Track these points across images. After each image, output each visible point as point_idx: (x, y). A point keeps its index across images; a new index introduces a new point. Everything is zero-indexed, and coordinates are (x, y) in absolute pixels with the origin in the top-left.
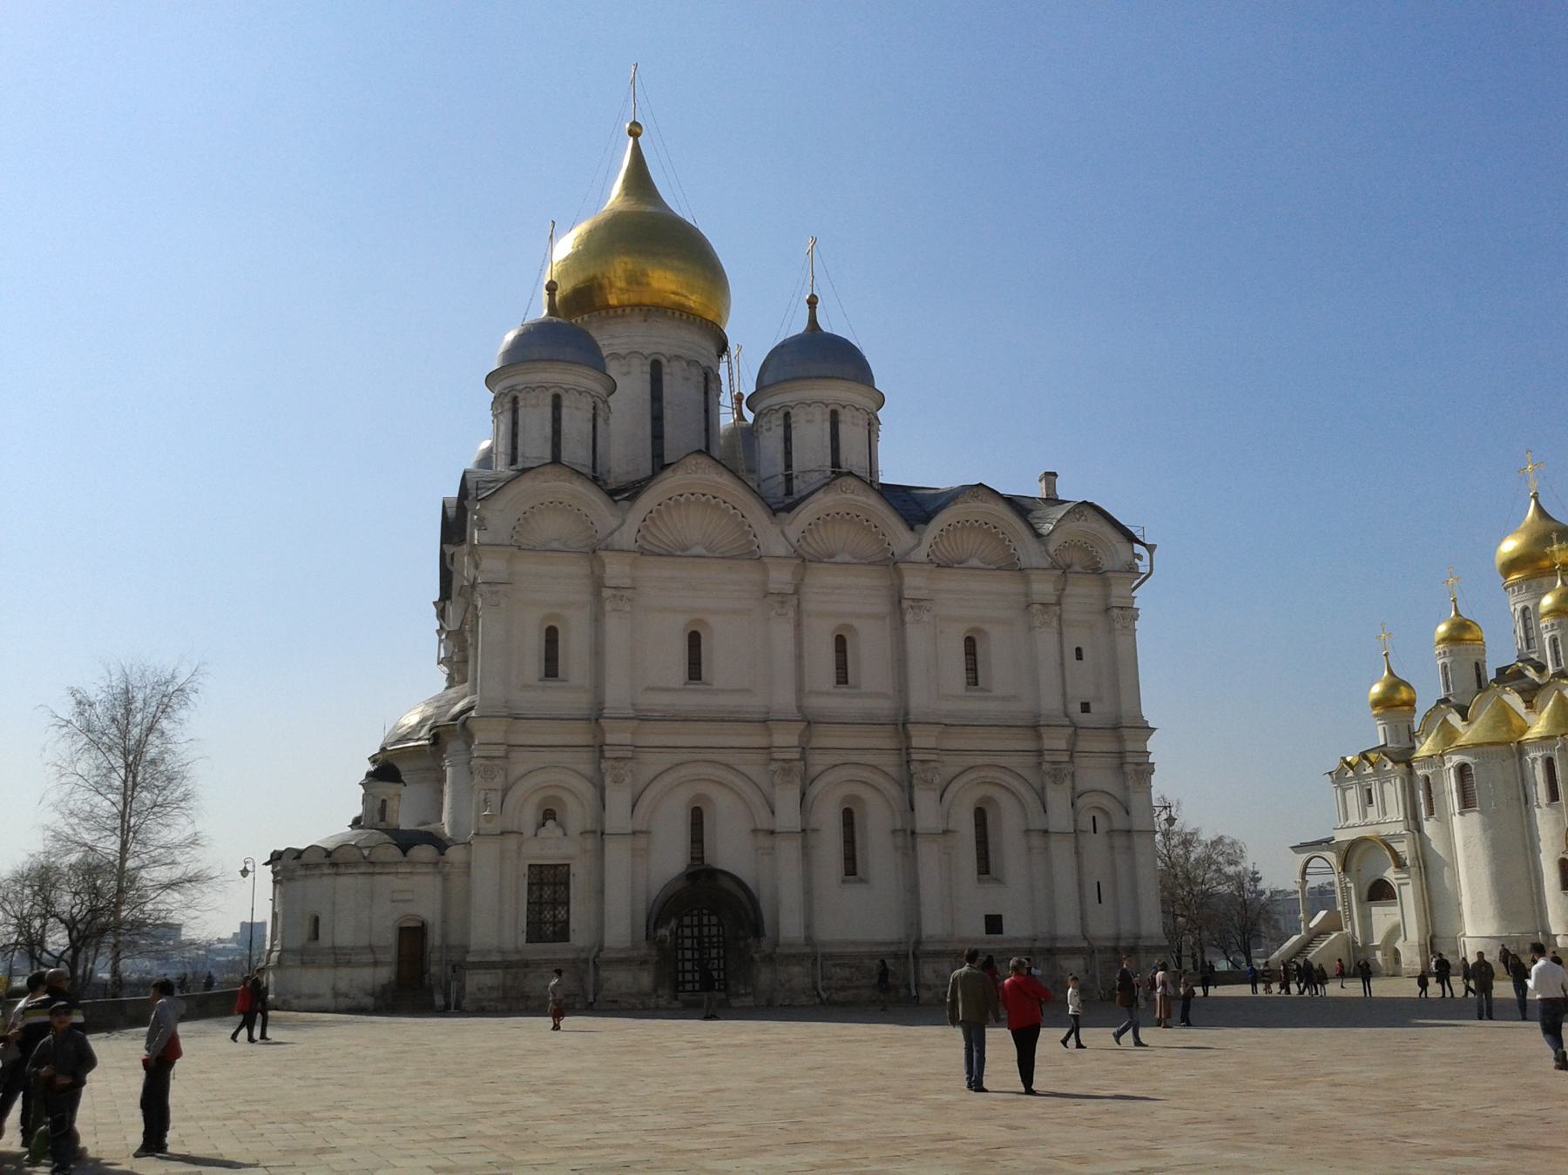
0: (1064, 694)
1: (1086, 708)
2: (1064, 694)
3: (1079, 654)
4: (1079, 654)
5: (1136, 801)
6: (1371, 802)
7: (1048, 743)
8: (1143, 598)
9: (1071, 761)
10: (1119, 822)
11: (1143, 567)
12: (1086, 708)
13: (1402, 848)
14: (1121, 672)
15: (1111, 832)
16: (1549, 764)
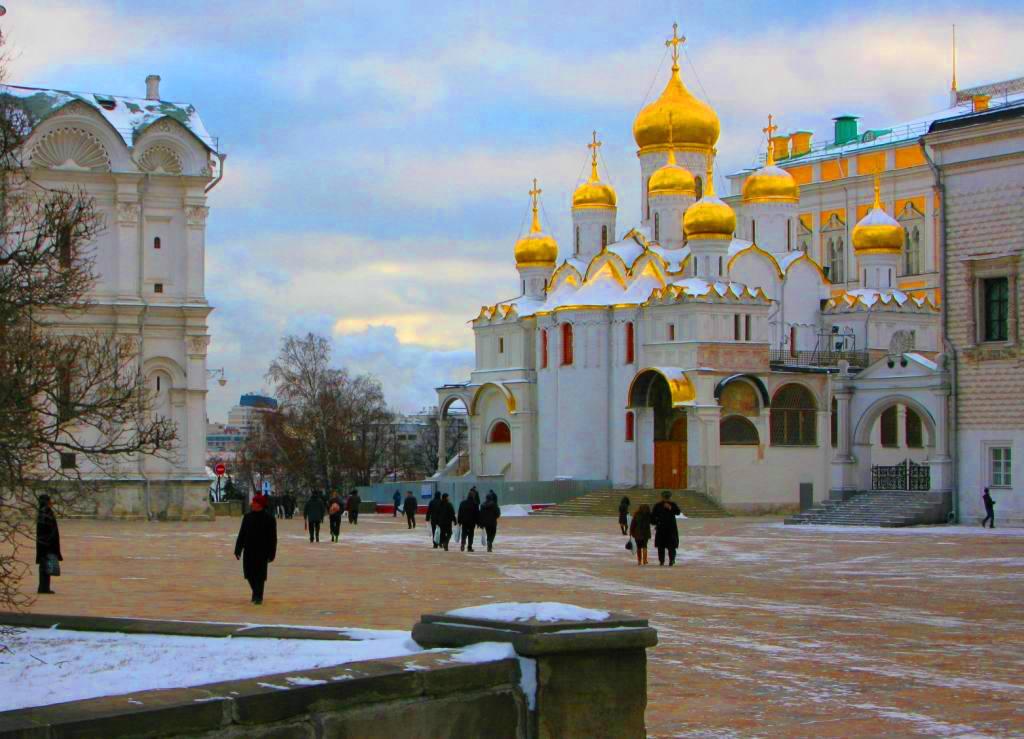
0: (140, 278)
1: (159, 288)
2: (140, 278)
3: (157, 243)
4: (157, 243)
5: (194, 365)
6: (502, 351)
7: (121, 320)
8: (214, 198)
9: (140, 334)
10: (177, 383)
11: (216, 175)
12: (159, 288)
13: (518, 395)
14: (190, 262)
15: (171, 390)
16: (630, 326)
